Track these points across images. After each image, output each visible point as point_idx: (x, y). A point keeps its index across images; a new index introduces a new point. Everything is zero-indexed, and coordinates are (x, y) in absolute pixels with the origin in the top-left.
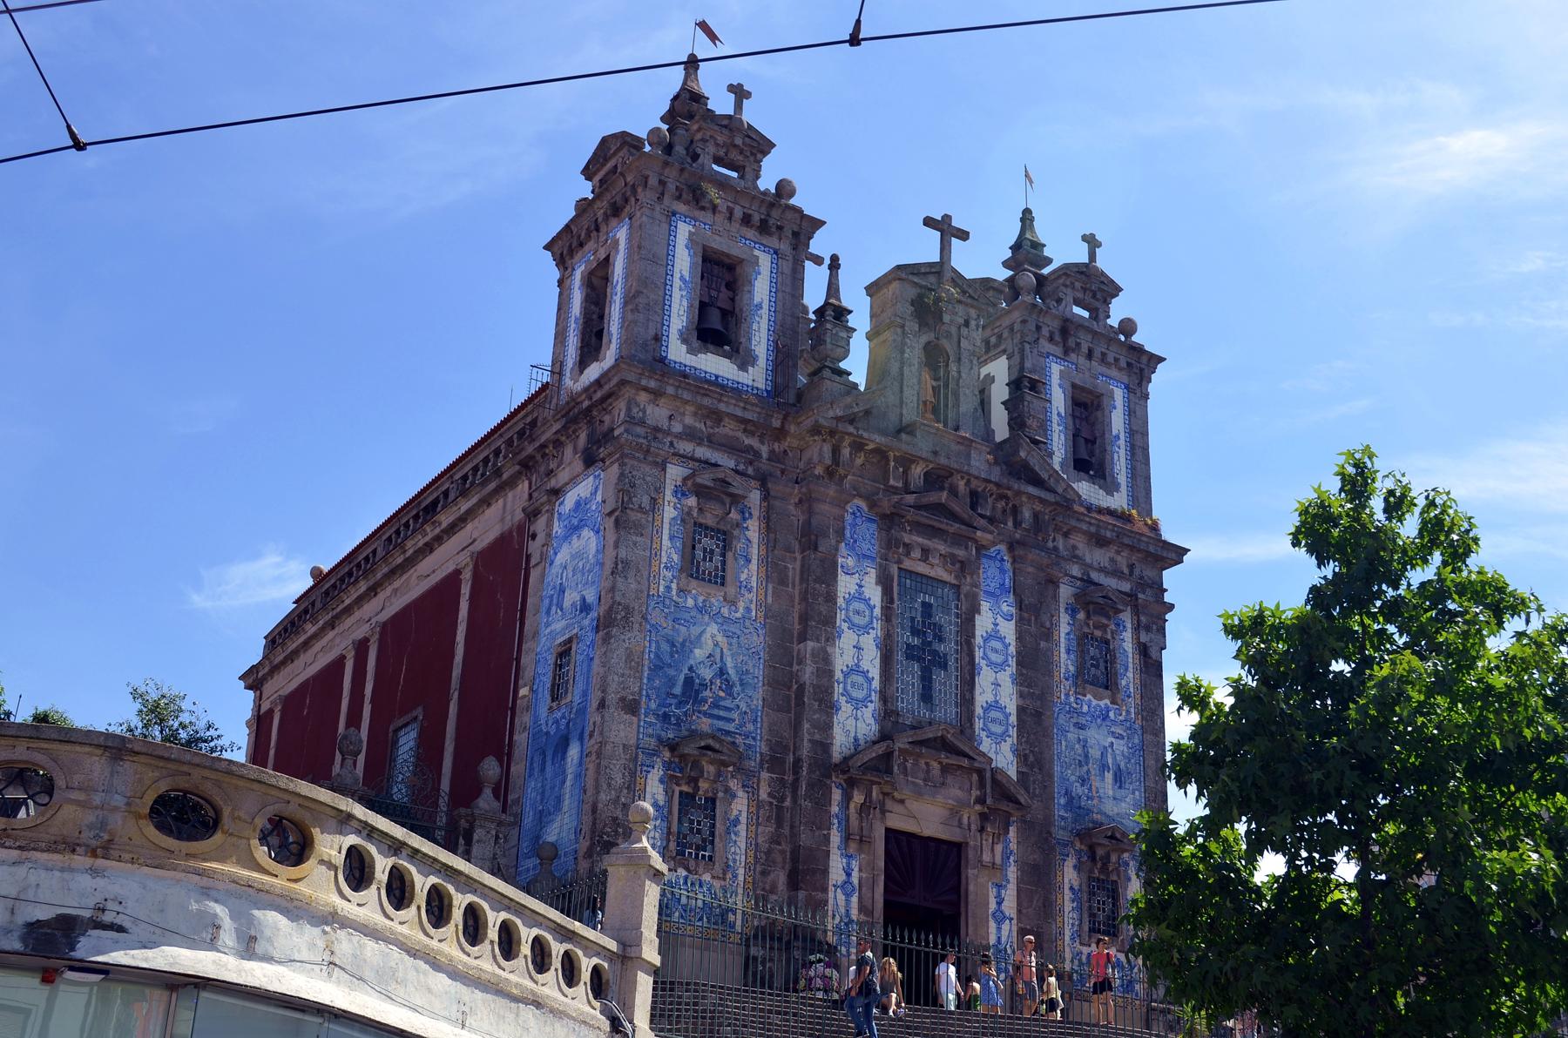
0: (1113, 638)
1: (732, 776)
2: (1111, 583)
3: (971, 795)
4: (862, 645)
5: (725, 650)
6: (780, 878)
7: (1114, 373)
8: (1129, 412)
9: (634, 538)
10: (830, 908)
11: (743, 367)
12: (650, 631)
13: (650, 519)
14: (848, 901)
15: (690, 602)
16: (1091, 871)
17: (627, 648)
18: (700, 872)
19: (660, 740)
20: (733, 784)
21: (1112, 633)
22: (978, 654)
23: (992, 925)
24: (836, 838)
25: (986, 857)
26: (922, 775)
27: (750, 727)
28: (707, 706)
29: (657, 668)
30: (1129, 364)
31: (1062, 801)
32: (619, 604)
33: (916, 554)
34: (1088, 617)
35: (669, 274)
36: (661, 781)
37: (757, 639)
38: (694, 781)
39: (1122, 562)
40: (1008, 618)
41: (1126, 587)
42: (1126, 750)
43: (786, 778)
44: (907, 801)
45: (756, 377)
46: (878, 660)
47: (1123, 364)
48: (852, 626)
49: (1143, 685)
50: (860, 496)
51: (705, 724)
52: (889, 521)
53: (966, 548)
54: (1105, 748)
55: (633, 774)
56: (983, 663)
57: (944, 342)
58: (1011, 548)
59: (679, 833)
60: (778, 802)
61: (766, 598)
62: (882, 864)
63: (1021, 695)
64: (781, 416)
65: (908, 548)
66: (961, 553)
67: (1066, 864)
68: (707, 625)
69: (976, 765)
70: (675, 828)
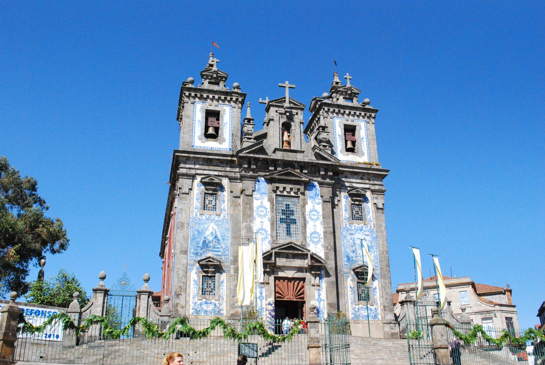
3: (304, 263)
4: (263, 221)
5: (217, 230)
9: (184, 201)
14: (261, 302)
17: (183, 235)
19: (195, 261)
22: (307, 218)
28: (211, 248)
29: (194, 239)
30: (365, 114)
31: (346, 259)
32: (180, 222)
33: (281, 189)
36: (196, 273)
37: (229, 226)
40: (319, 204)
41: (367, 186)
42: (370, 239)
48: (259, 216)
49: (377, 217)
51: (209, 254)
56: (309, 220)
63: (325, 228)
65: (278, 188)
67: (348, 279)
68: (210, 223)
69: (304, 253)
70: (201, 287)
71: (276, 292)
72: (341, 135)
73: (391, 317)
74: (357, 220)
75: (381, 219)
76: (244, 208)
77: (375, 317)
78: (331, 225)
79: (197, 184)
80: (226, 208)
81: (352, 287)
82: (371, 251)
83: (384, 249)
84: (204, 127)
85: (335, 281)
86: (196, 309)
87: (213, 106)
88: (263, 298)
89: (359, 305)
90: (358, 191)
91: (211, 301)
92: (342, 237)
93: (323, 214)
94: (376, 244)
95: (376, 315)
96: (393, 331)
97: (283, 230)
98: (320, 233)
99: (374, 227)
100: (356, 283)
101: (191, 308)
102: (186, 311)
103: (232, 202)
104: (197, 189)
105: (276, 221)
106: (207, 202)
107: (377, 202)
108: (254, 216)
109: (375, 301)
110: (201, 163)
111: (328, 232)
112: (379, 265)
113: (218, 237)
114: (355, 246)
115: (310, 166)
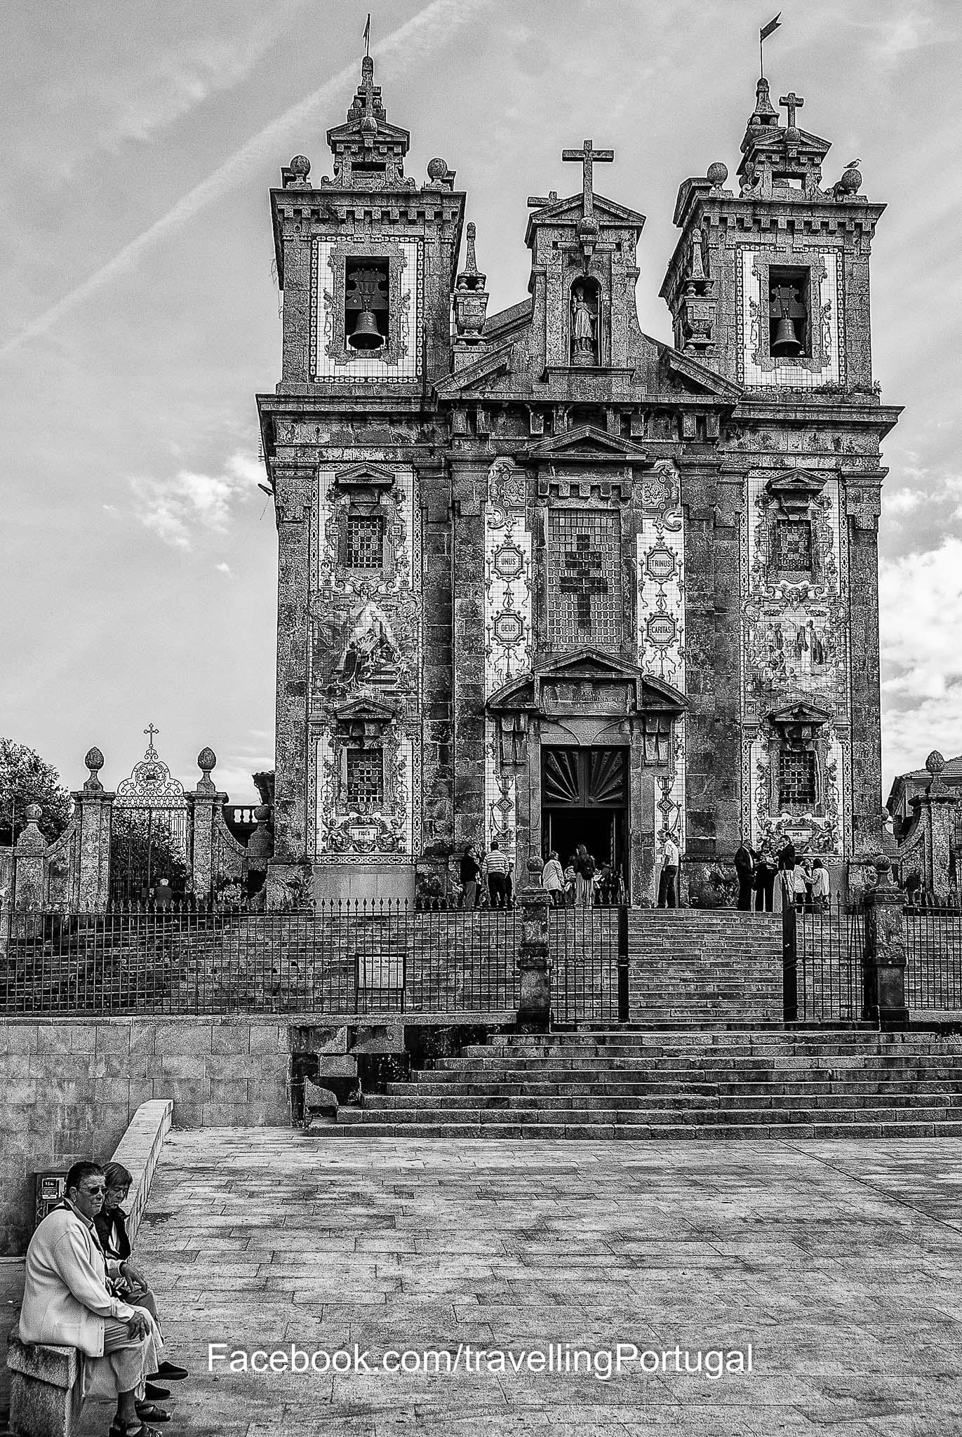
2: (812, 463)
6: (446, 804)
7: (822, 240)
8: (844, 275)
14: (505, 817)
15: (349, 589)
19: (327, 710)
21: (813, 513)
23: (659, 814)
24: (491, 764)
25: (651, 757)
27: (412, 684)
29: (321, 651)
30: (841, 225)
31: (749, 688)
35: (313, 298)
36: (331, 745)
37: (415, 607)
38: (359, 739)
41: (830, 463)
45: (407, 367)
46: (530, 599)
48: (501, 575)
49: (852, 558)
50: (505, 455)
51: (366, 691)
53: (621, 474)
63: (690, 600)
70: (345, 780)
71: (546, 786)
72: (758, 303)
80: (410, 559)
86: (333, 840)
87: (365, 242)
89: (780, 816)
90: (798, 480)
91: (373, 817)
92: (742, 623)
95: (828, 841)
99: (842, 589)
100: (775, 753)
103: (426, 539)
104: (327, 508)
108: (486, 577)
110: (335, 428)
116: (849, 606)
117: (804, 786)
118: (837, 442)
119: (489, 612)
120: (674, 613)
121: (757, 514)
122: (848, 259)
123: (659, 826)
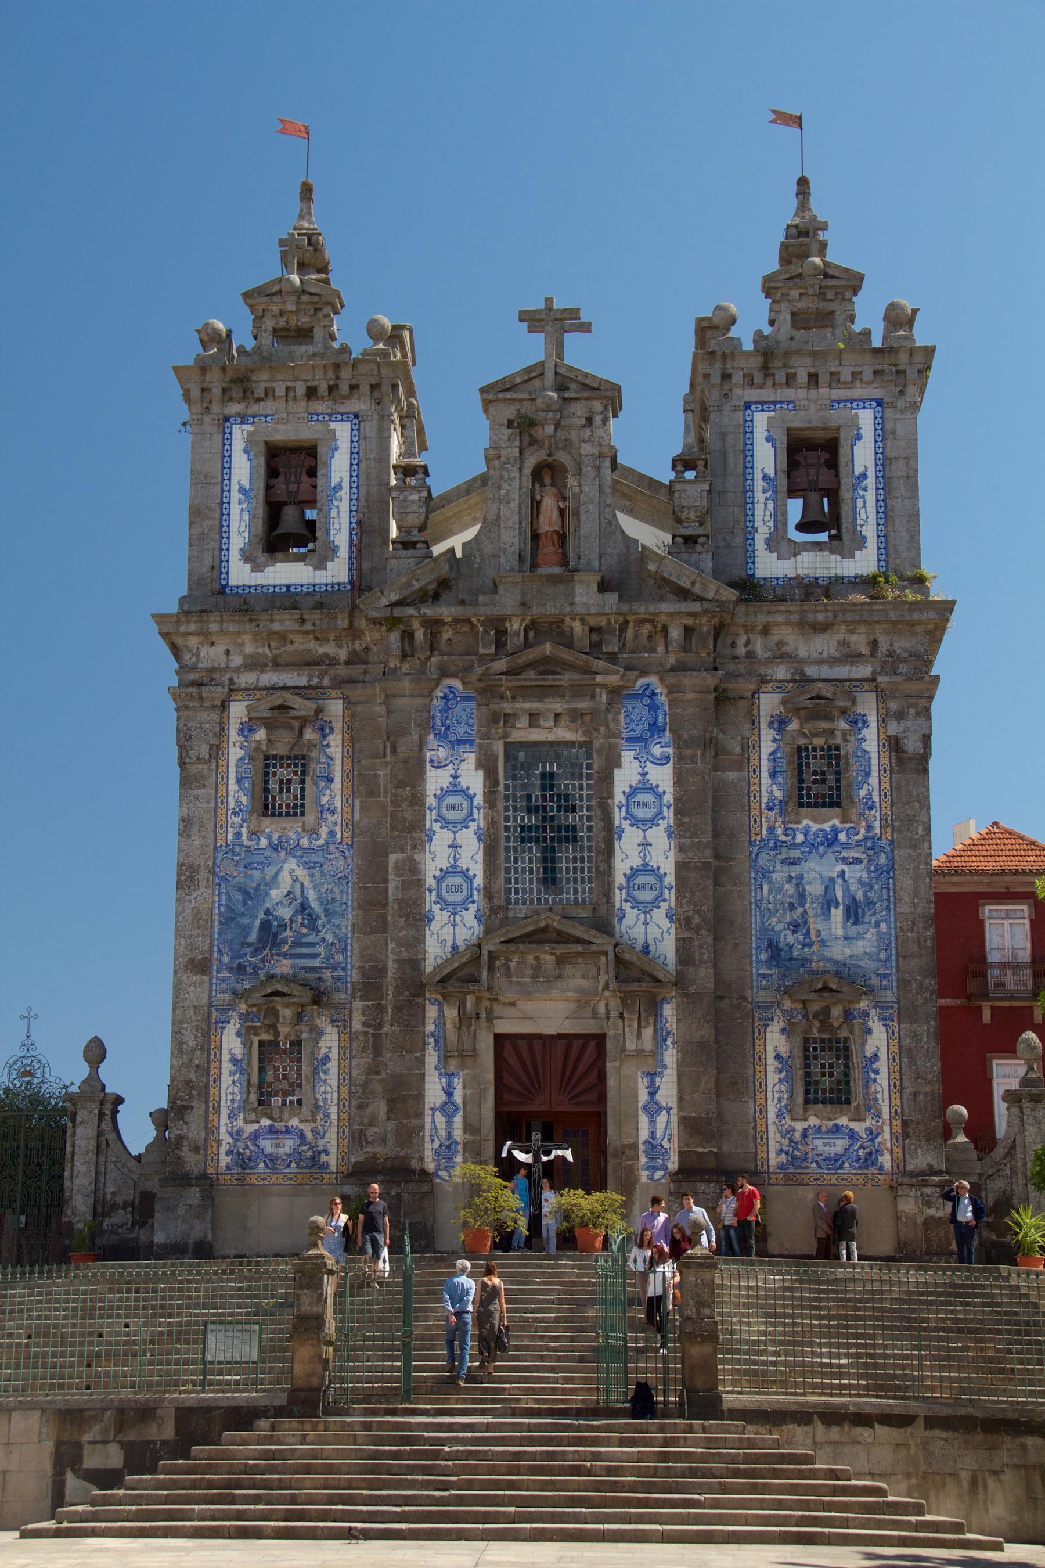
0: (846, 740)
1: (319, 1014)
2: (842, 672)
3: (598, 981)
4: (459, 842)
5: (305, 884)
7: (859, 391)
9: (195, 792)
10: (427, 1133)
11: (320, 566)
12: (219, 884)
13: (214, 767)
14: (449, 1123)
15: (264, 843)
16: (808, 1030)
17: (193, 908)
18: (286, 1116)
19: (235, 993)
20: (323, 1022)
21: (844, 734)
22: (618, 815)
24: (431, 1058)
26: (529, 972)
27: (340, 958)
28: (287, 947)
29: (230, 918)
31: (764, 956)
32: (183, 864)
33: (524, 722)
34: (801, 724)
35: (225, 491)
36: (238, 1034)
38: (273, 1028)
39: (859, 641)
40: (662, 761)
41: (864, 671)
42: (865, 875)
43: (383, 1002)
44: (518, 1003)
46: (481, 853)
47: (868, 375)
48: (446, 824)
50: (451, 676)
51: (284, 967)
52: (488, 691)
53: (593, 696)
54: (832, 880)
55: (207, 1034)
56: (626, 824)
57: (562, 457)
58: (661, 680)
59: (261, 1086)
60: (375, 1029)
61: (353, 817)
62: (490, 1076)
63: (681, 849)
64: (346, 615)
65: (509, 718)
66: (584, 705)
67: (769, 1029)
68: (285, 861)
69: (594, 948)
70: (255, 1079)
72: (772, 475)
73: (929, 1159)
74: (816, 805)
75: (915, 793)
76: (396, 802)
77: (869, 1162)
78: (706, 838)
79: (238, 726)
80: (338, 804)
81: (785, 1055)
82: (866, 919)
83: (919, 911)
84: (261, 512)
85: (713, 1038)
86: (239, 1154)
88: (457, 1109)
89: (806, 1120)
92: (753, 875)
93: (677, 800)
94: (885, 897)
95: (870, 1154)
96: (931, 1212)
97: (531, 869)
98: (662, 871)
100: (798, 1041)
101: (223, 1149)
102: (209, 1162)
105: (508, 839)
106: (274, 786)
107: (901, 729)
109: (870, 1106)
111: (692, 865)
112: (894, 971)
113: (311, 907)
114: (803, 906)
115: (631, 624)
116: (892, 851)
117: (839, 1082)
118: (874, 644)
119: (431, 870)
120: (662, 866)
121: (771, 737)
122: (889, 413)
123: (644, 1135)
